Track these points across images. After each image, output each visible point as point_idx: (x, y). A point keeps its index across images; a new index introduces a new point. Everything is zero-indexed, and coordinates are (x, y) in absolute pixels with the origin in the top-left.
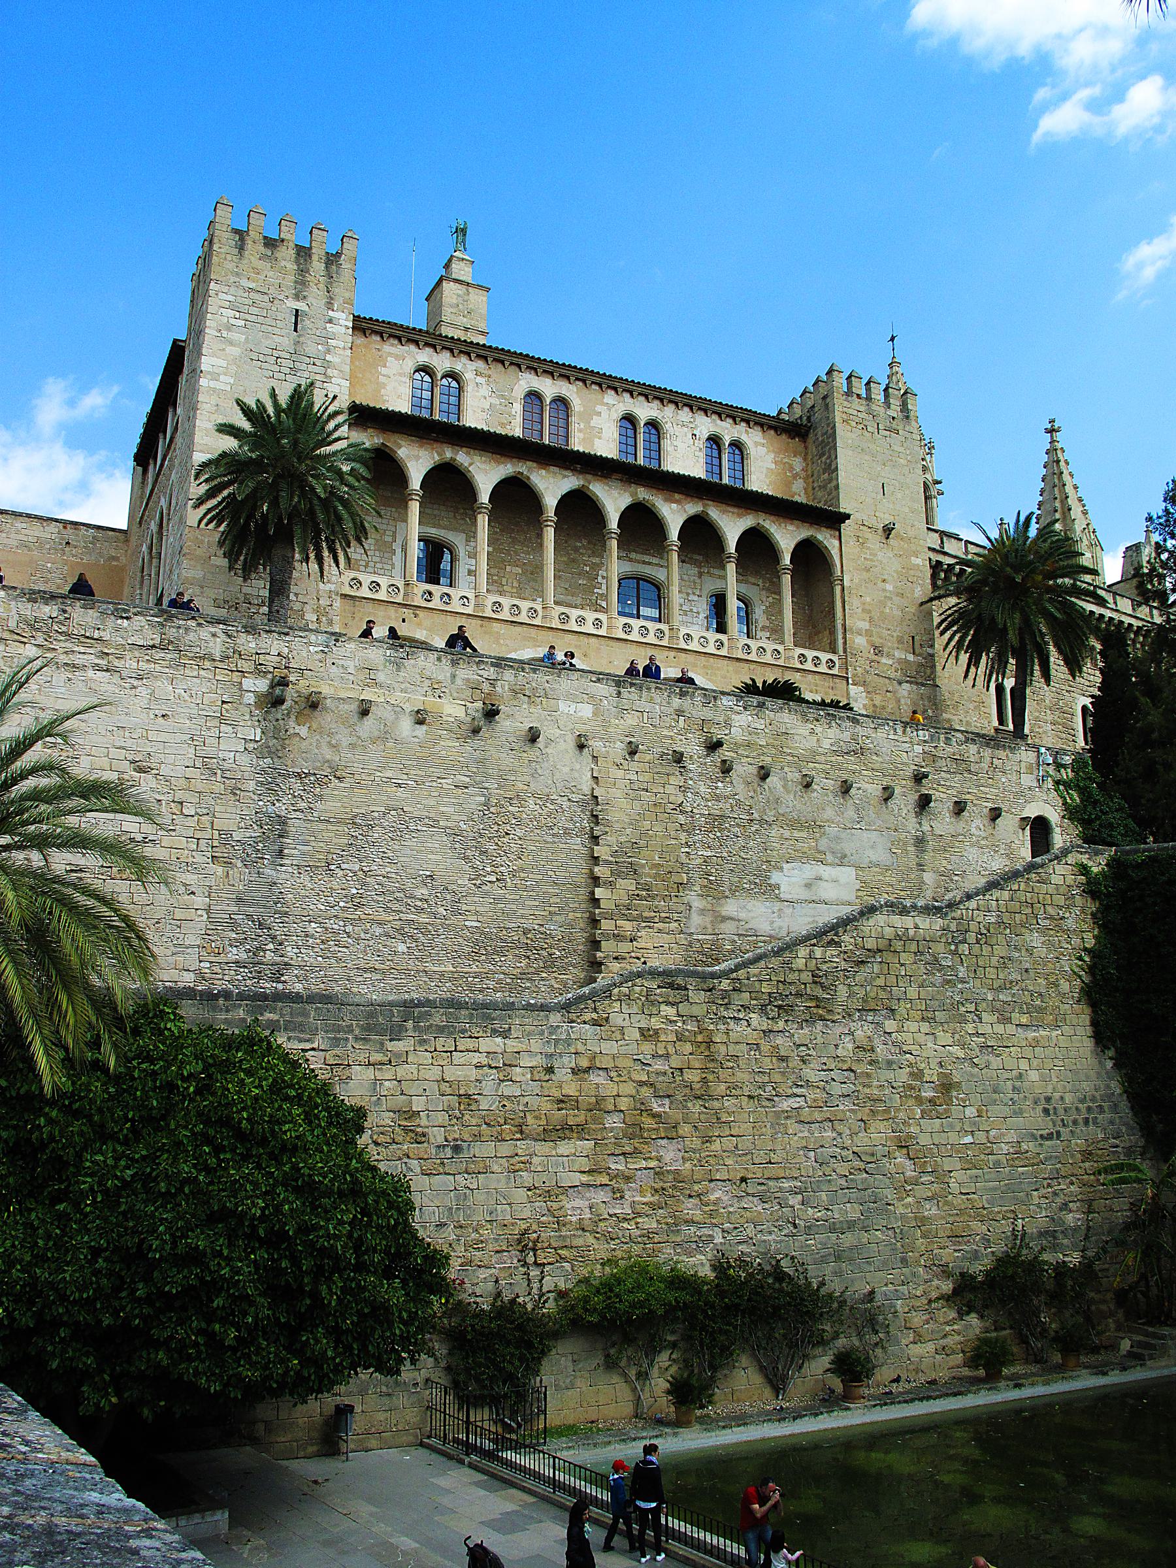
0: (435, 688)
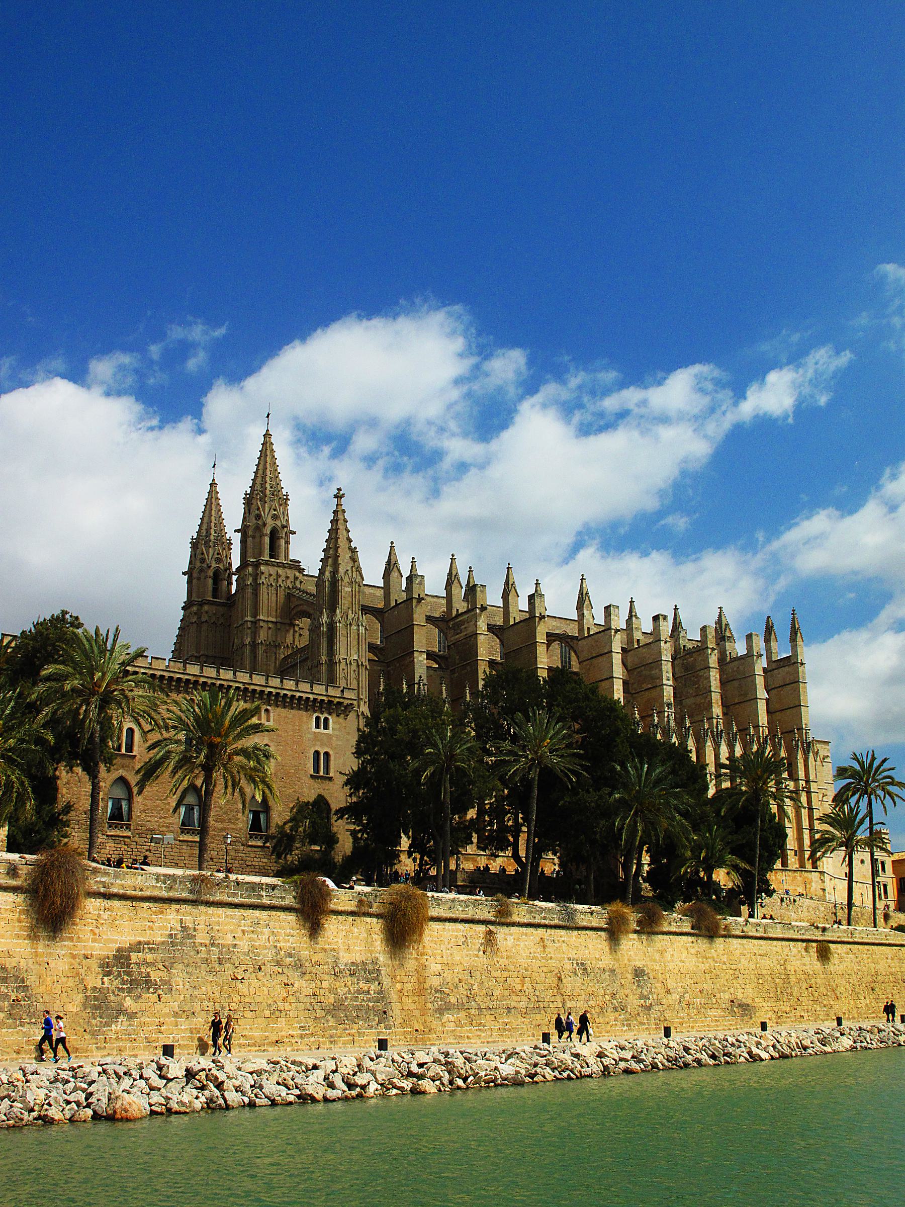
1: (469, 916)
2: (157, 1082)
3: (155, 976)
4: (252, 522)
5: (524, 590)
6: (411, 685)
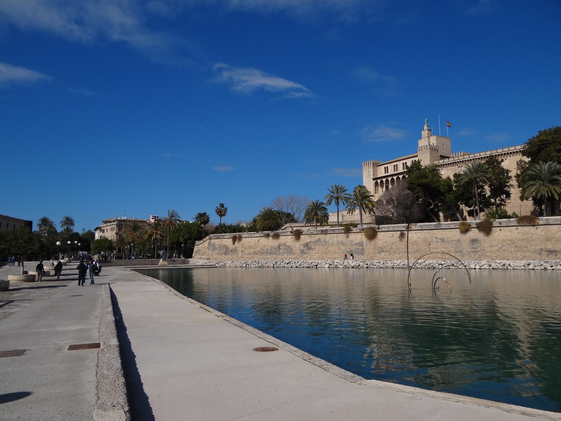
1: (395, 229)
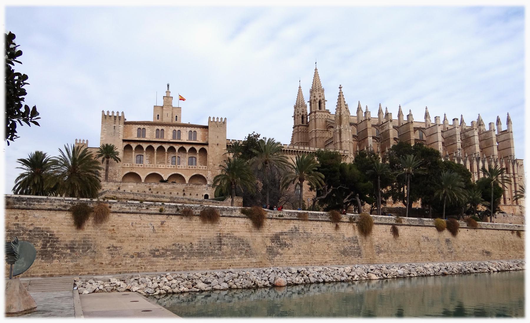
0: (112, 186)
1: (387, 222)
2: (288, 274)
3: (287, 242)
4: (313, 98)
5: (405, 113)
6: (367, 148)
